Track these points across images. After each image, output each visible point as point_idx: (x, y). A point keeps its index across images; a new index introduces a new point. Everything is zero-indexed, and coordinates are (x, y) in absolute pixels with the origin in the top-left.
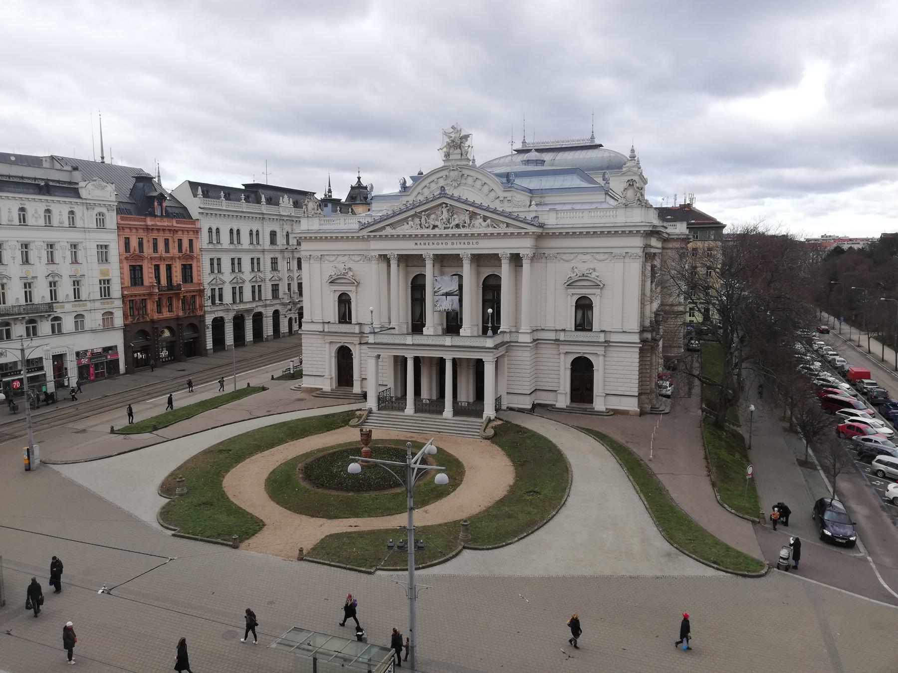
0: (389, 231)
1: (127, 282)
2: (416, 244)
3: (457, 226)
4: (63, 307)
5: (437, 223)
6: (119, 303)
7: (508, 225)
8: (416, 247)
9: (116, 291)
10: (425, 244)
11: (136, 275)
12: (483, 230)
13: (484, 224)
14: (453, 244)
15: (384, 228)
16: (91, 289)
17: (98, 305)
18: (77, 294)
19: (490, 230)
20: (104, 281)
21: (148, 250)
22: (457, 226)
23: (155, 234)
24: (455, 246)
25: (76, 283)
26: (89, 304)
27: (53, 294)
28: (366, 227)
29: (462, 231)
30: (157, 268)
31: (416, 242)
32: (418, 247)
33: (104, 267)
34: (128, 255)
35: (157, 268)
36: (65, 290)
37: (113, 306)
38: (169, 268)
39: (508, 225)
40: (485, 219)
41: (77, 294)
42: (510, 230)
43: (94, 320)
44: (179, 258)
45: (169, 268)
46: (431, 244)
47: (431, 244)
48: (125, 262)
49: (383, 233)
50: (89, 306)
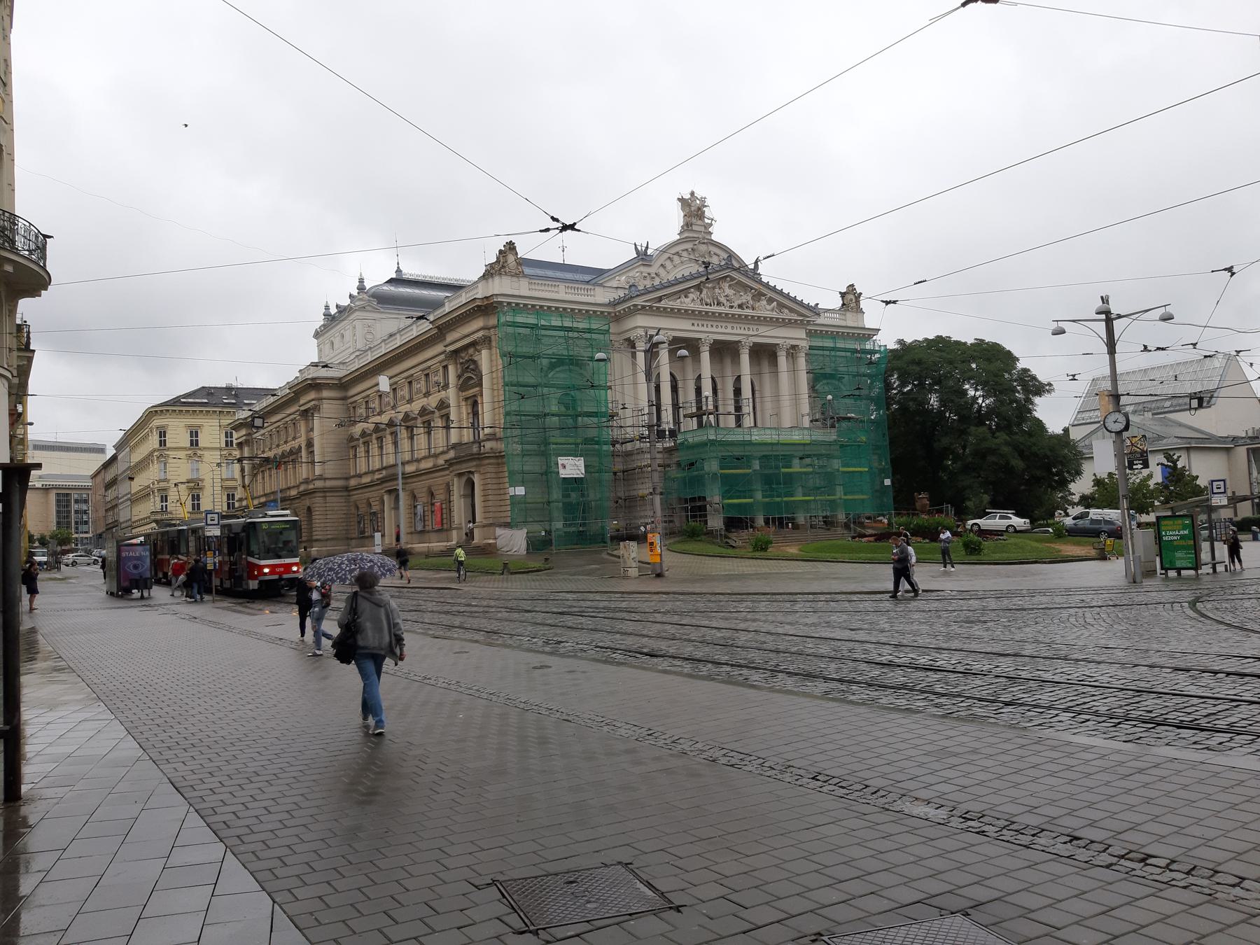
0: (663, 304)
2: (693, 324)
3: (740, 306)
5: (723, 300)
7: (792, 310)
8: (693, 328)
10: (703, 325)
12: (768, 314)
13: (768, 307)
14: (733, 328)
15: (660, 299)
19: (774, 315)
22: (740, 306)
24: (735, 331)
28: (643, 294)
29: (749, 312)
31: (693, 322)
32: (695, 328)
39: (792, 310)
40: (770, 300)
42: (795, 317)
46: (709, 326)
47: (709, 326)
49: (663, 304)
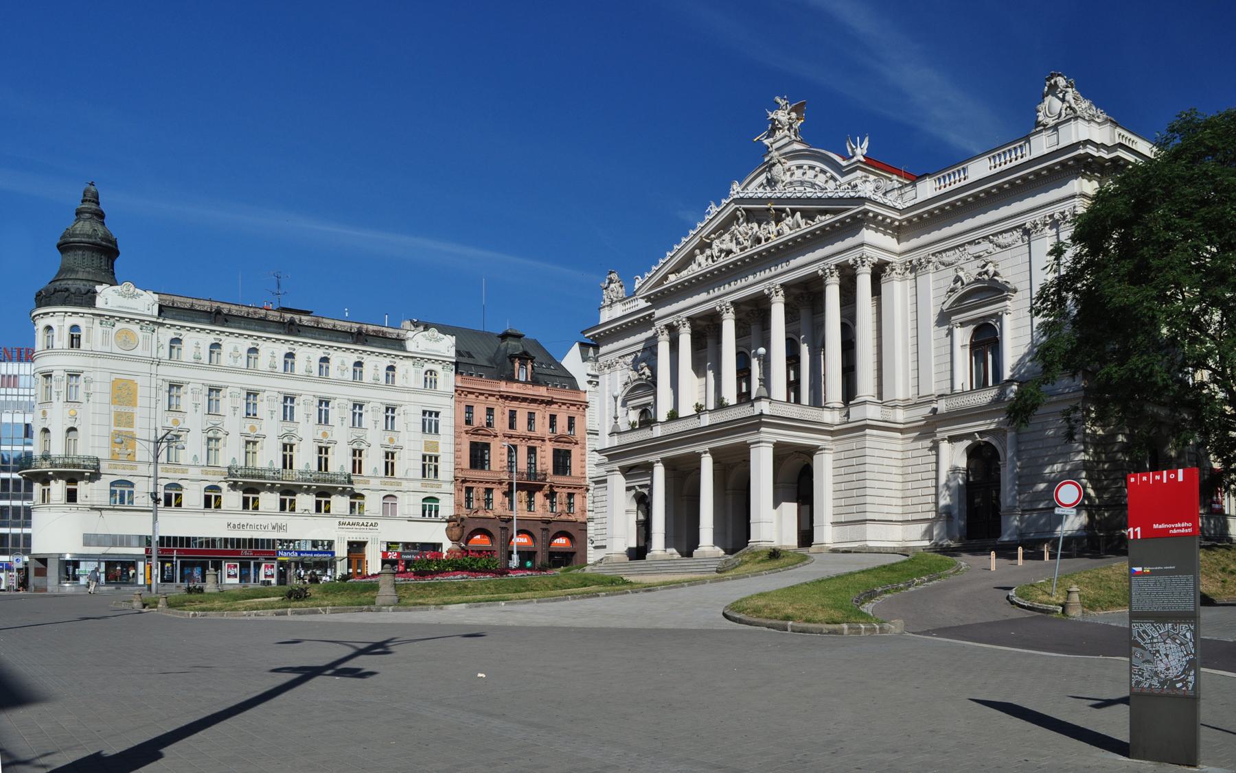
1: (466, 463)
4: (367, 482)
6: (450, 488)
9: (446, 469)
11: (479, 456)
16: (409, 464)
17: (417, 485)
18: (389, 469)
20: (430, 457)
21: (501, 423)
23: (514, 405)
25: (389, 455)
26: (404, 483)
27: (357, 466)
30: (512, 450)
33: (431, 438)
34: (469, 428)
35: (512, 450)
36: (373, 462)
37: (438, 490)
38: (532, 451)
41: (389, 469)
43: (410, 504)
44: (550, 440)
45: (532, 451)
48: (464, 435)
50: (405, 485)
